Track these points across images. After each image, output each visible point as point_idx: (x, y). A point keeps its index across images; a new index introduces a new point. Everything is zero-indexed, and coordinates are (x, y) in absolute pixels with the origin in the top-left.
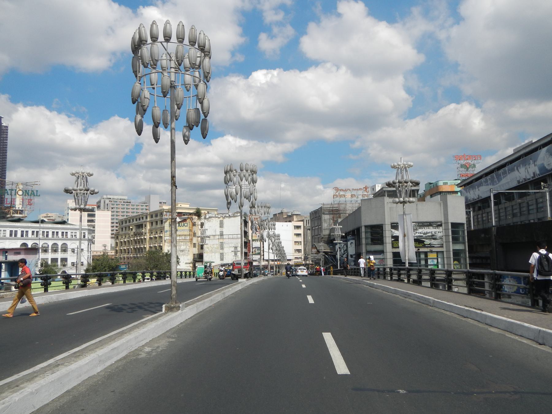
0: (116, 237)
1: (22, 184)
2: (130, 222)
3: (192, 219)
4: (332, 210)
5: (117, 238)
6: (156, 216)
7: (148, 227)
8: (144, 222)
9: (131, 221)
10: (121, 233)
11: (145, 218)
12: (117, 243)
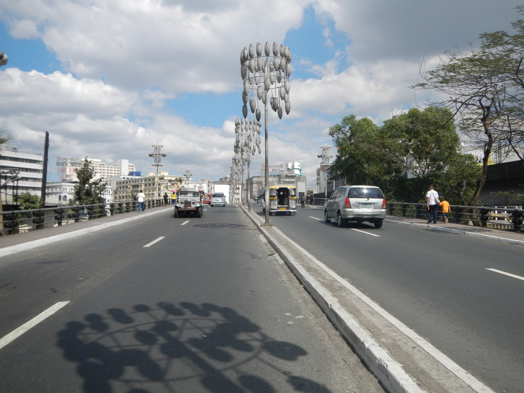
0: (115, 193)
1: (70, 159)
2: (127, 183)
3: (177, 184)
4: (258, 182)
5: (116, 193)
6: (149, 180)
7: (143, 187)
8: (140, 184)
9: (129, 182)
10: (119, 190)
11: (140, 181)
12: (116, 197)
